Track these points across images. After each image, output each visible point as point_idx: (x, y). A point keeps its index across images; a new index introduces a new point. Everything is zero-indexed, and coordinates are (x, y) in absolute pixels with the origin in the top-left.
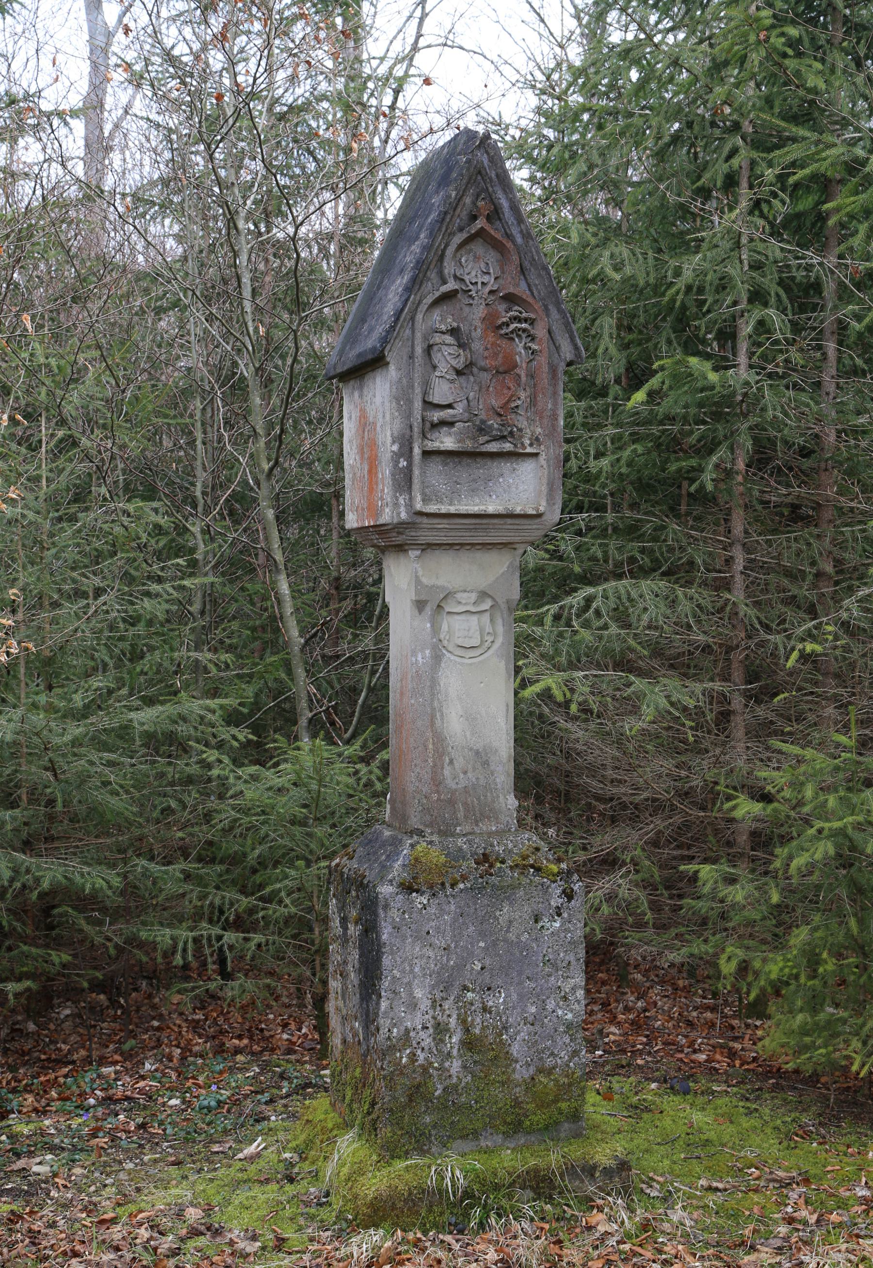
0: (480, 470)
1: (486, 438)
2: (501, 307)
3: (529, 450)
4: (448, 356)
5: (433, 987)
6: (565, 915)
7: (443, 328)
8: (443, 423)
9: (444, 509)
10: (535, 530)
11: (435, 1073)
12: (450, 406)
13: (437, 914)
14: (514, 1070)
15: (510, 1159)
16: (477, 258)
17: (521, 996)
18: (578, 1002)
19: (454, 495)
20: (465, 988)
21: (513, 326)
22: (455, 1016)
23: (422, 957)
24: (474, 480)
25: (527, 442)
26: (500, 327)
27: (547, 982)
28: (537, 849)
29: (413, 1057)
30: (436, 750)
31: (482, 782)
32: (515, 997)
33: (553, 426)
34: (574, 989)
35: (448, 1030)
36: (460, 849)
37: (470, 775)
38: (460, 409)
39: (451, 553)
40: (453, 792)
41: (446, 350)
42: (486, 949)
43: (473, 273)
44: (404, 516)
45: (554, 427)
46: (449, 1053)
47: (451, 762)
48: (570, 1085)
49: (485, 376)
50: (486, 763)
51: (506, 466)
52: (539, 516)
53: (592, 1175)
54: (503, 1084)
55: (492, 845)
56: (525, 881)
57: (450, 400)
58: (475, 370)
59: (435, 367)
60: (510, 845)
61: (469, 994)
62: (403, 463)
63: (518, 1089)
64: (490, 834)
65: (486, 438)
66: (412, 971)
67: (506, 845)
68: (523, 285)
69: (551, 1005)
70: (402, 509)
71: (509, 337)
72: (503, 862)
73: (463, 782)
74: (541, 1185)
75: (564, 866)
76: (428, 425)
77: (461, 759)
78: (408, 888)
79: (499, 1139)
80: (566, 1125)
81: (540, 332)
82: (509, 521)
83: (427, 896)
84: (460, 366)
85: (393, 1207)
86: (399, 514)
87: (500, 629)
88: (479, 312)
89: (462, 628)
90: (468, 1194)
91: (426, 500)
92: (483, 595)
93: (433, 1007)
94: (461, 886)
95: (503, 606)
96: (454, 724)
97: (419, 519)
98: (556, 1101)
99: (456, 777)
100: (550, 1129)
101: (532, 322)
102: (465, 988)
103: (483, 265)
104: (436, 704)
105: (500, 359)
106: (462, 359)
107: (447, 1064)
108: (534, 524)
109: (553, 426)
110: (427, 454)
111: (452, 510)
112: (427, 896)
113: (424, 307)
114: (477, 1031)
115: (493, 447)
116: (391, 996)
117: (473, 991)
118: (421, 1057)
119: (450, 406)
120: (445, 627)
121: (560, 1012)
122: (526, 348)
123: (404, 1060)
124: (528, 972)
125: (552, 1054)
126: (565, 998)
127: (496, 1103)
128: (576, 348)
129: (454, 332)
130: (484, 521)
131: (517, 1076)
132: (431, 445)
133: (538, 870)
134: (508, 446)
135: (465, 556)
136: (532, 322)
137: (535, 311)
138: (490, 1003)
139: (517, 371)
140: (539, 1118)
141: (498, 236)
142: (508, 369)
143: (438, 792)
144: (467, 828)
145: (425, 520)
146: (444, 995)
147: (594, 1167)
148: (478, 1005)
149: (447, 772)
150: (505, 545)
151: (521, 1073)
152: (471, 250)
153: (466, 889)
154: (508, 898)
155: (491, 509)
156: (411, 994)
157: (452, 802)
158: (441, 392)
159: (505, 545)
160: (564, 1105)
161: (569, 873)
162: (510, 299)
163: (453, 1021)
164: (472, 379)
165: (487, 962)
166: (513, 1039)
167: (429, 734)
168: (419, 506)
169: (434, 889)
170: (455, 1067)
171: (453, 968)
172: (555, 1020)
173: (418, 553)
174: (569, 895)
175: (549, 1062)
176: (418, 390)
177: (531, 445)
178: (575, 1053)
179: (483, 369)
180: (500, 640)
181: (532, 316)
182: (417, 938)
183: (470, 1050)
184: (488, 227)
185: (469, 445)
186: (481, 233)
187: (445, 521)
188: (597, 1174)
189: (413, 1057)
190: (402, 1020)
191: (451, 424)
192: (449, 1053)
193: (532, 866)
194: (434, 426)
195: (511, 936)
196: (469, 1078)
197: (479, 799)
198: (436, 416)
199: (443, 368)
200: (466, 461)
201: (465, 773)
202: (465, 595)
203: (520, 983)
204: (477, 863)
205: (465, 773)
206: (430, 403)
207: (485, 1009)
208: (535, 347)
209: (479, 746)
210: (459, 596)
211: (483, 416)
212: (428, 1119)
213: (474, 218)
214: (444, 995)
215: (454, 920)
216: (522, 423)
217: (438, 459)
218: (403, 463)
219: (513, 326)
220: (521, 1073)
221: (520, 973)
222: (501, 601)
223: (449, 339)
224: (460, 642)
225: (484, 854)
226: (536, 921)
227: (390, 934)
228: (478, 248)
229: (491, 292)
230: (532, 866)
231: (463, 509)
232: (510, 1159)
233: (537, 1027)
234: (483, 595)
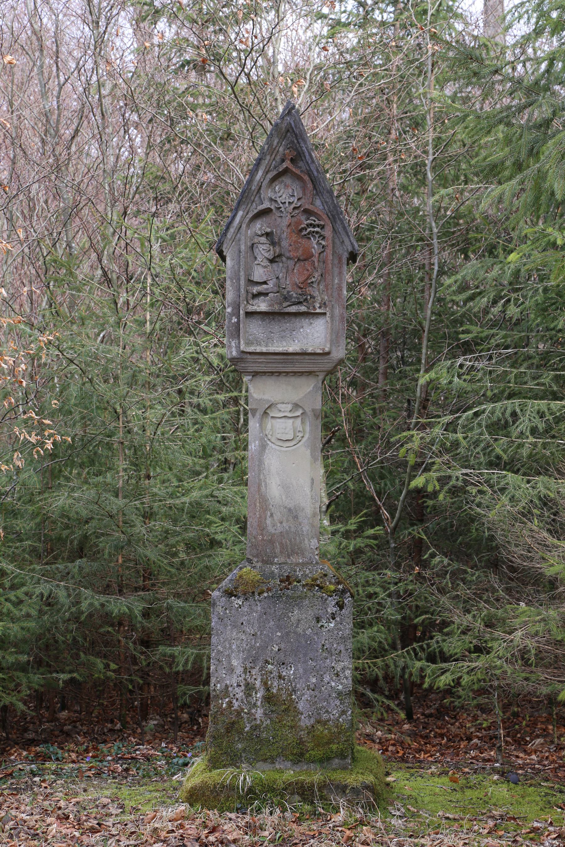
0: (287, 324)
1: (288, 303)
2: (303, 218)
3: (318, 311)
4: (264, 250)
5: (245, 659)
6: (338, 619)
7: (259, 233)
8: (259, 294)
9: (258, 349)
11: (245, 716)
12: (265, 283)
13: (250, 612)
14: (300, 719)
15: (289, 774)
16: (286, 186)
17: (305, 671)
18: (347, 678)
19: (269, 340)
20: (267, 662)
21: (309, 230)
22: (259, 680)
23: (238, 639)
24: (283, 331)
26: (301, 230)
27: (324, 662)
28: (325, 575)
29: (230, 704)
30: (261, 507)
31: (293, 529)
32: (301, 671)
33: (339, 294)
34: (343, 669)
35: (255, 688)
36: (273, 572)
37: (284, 524)
38: (271, 284)
39: (274, 378)
40: (273, 535)
42: (281, 637)
43: (284, 196)
44: (234, 353)
46: (255, 704)
47: (272, 515)
48: (339, 733)
49: (291, 263)
50: (296, 517)
51: (305, 322)
52: (328, 353)
53: (344, 792)
54: (292, 727)
55: (295, 571)
56: (310, 594)
57: (264, 279)
59: (256, 258)
60: (308, 571)
61: (270, 666)
62: (234, 320)
63: (302, 733)
64: (297, 564)
65: (288, 303)
66: (230, 647)
67: (305, 572)
68: (318, 202)
69: (327, 678)
70: (234, 349)
72: (298, 582)
73: (279, 528)
74: (305, 792)
75: (340, 587)
77: (279, 514)
78: (229, 594)
79: (289, 764)
80: (337, 761)
81: (328, 232)
82: (307, 357)
83: (242, 599)
84: (271, 257)
85: (203, 794)
86: (231, 352)
87: (308, 428)
88: (286, 221)
89: (281, 426)
90: (251, 790)
91: (248, 343)
92: (296, 406)
93: (245, 672)
94: (266, 595)
95: (309, 413)
96: (274, 491)
97: (245, 356)
98: (328, 743)
99: (275, 525)
100: (325, 760)
101: (323, 227)
102: (267, 662)
103: (290, 191)
104: (262, 476)
105: (300, 252)
106: (272, 252)
107: (253, 711)
108: (325, 359)
110: (249, 314)
111: (264, 350)
112: (242, 599)
113: (247, 220)
114: (275, 691)
115: (293, 309)
116: (217, 663)
117: (272, 664)
118: (236, 704)
119: (265, 283)
120: (269, 426)
121: (333, 684)
122: (318, 243)
123: (224, 705)
124: (311, 655)
125: (327, 711)
126: (337, 675)
127: (287, 740)
128: (352, 244)
130: (290, 357)
131: (302, 724)
132: (250, 309)
133: (321, 588)
134: (303, 309)
135: (283, 379)
136: (323, 227)
137: (323, 220)
138: (284, 674)
139: (313, 259)
140: (317, 753)
141: (298, 172)
142: (307, 257)
143: (262, 535)
144: (282, 560)
145: (249, 356)
146: (252, 665)
147: (346, 786)
148: (275, 674)
149: (269, 521)
151: (305, 722)
153: (268, 596)
154: (297, 605)
155: (291, 350)
156: (229, 662)
157: (271, 542)
158: (258, 274)
160: (334, 747)
161: (344, 592)
162: (308, 212)
163: (258, 683)
164: (281, 265)
165: (283, 646)
166: (299, 698)
167: (257, 496)
168: (242, 348)
169: (247, 595)
170: (259, 713)
171: (259, 648)
172: (329, 689)
173: (250, 377)
174: (341, 606)
175: (325, 717)
176: (242, 273)
177: (320, 307)
178: (343, 712)
179: (288, 258)
180: (307, 436)
181: (322, 223)
182: (234, 626)
183: (269, 703)
184: (291, 167)
185: (276, 308)
186: (286, 171)
188: (348, 791)
189: (230, 704)
190: (223, 679)
191: (266, 294)
192: (255, 704)
193: (318, 586)
194: (255, 296)
195: (300, 630)
196: (269, 722)
197: (290, 541)
199: (260, 258)
201: (281, 523)
202: (284, 405)
203: (305, 662)
204: (281, 581)
205: (281, 523)
207: (280, 677)
208: (323, 243)
209: (291, 505)
210: (279, 406)
211: (289, 288)
212: (240, 746)
213: (283, 161)
214: (252, 665)
215: (260, 617)
216: (316, 294)
217: (258, 317)
218: (234, 320)
219: (309, 230)
220: (305, 722)
221: (305, 655)
222: (308, 410)
223: (263, 239)
224: (279, 436)
225: (288, 577)
226: (318, 622)
227: (216, 622)
228: (287, 180)
229: (295, 208)
230: (318, 586)
231: (272, 349)
232: (289, 774)
233: (316, 693)
234: (296, 406)
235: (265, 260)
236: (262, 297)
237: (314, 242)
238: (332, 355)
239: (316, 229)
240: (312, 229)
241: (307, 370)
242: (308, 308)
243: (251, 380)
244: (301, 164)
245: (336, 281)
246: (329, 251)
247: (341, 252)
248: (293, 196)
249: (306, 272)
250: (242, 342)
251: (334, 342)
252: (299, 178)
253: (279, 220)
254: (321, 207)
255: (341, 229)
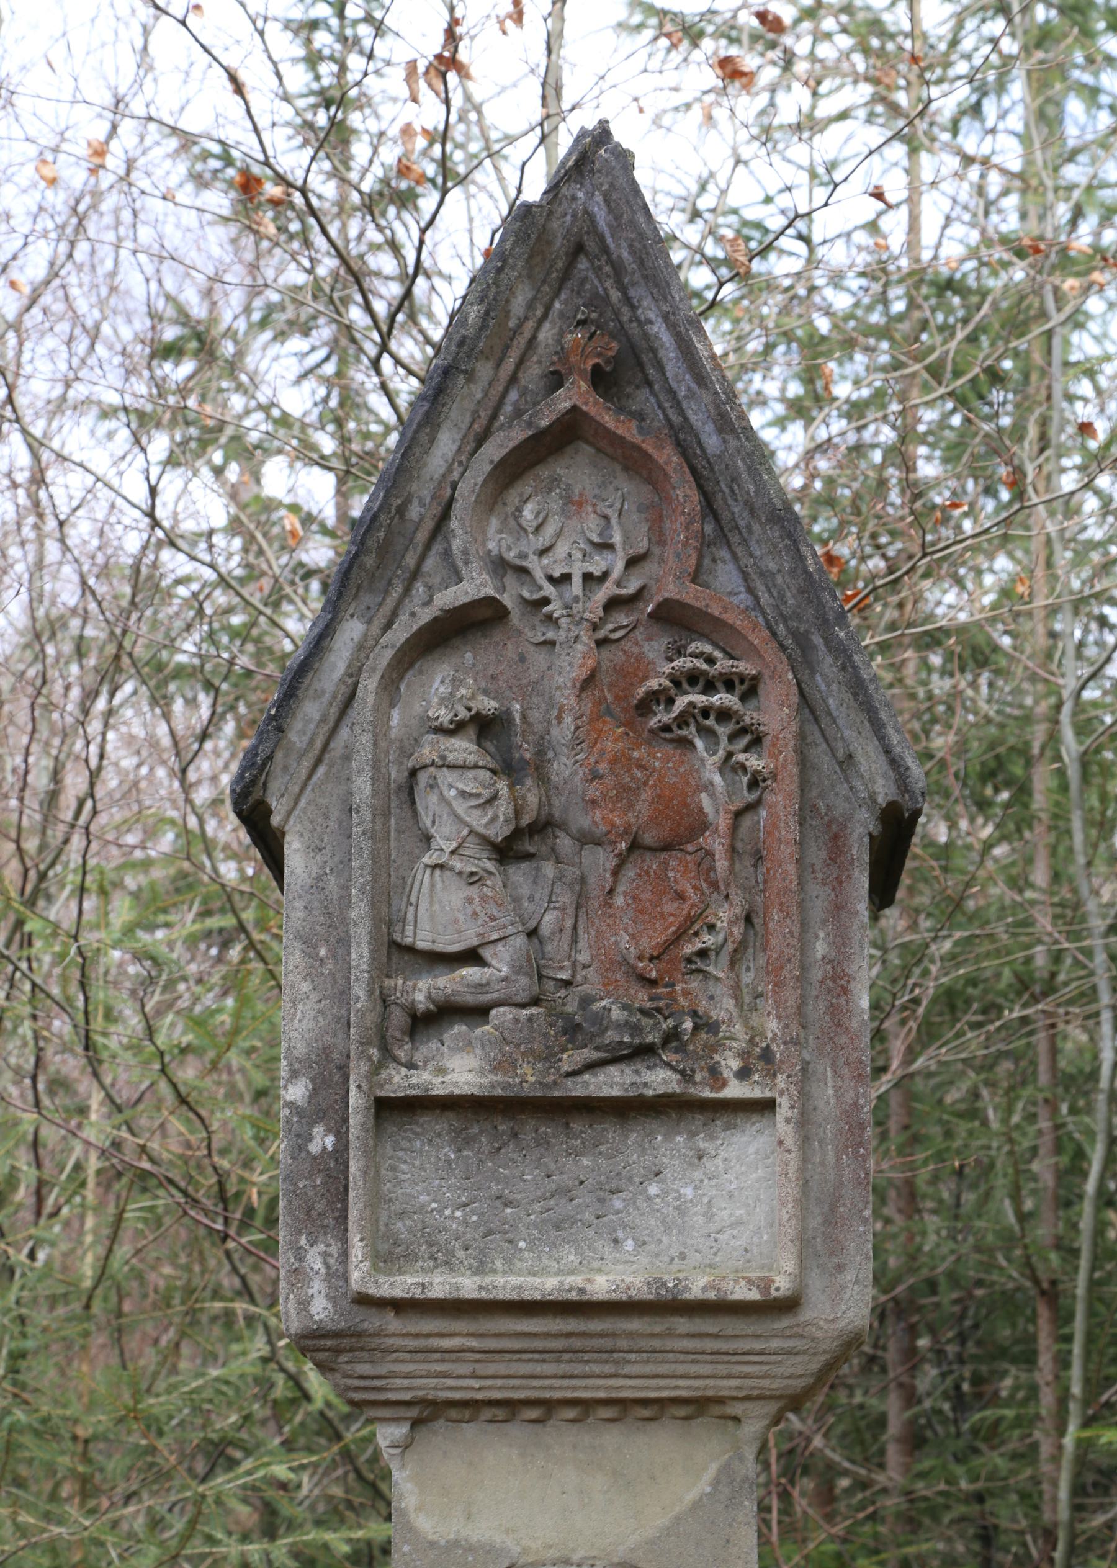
0: (581, 1157)
3: (735, 1090)
4: (462, 802)
9: (439, 1285)
10: (783, 1359)
12: (472, 957)
19: (491, 1241)
25: (731, 1063)
26: (644, 707)
33: (834, 1011)
38: (501, 963)
41: (452, 784)
43: (561, 550)
44: (320, 1308)
45: (838, 1015)
51: (670, 1145)
52: (788, 1305)
58: (564, 843)
59: (428, 838)
70: (317, 1286)
71: (674, 737)
76: (398, 1018)
81: (774, 713)
82: (683, 1324)
84: (499, 832)
88: (573, 661)
91: (386, 1258)
97: (372, 1321)
103: (592, 527)
105: (643, 807)
106: (503, 808)
108: (773, 1334)
109: (834, 1011)
110: (390, 1110)
111: (469, 1286)
115: (612, 1082)
119: (472, 957)
122: (729, 766)
128: (894, 762)
129: (484, 727)
130: (595, 1325)
132: (400, 1082)
134: (659, 1080)
135: (563, 1438)
136: (750, 688)
137: (754, 652)
141: (629, 431)
142: (676, 833)
145: (393, 1323)
150: (699, 1406)
152: (555, 480)
155: (601, 1286)
158: (441, 913)
159: (699, 1406)
162: (674, 618)
164: (549, 869)
168: (359, 1276)
173: (399, 1431)
176: (359, 911)
177: (743, 1074)
179: (586, 839)
181: (746, 667)
185: (528, 1078)
187: (461, 1325)
191: (479, 1013)
198: (424, 989)
200: (530, 1128)
206: (411, 950)
208: (754, 762)
213: (556, 380)
216: (723, 1008)
217: (438, 1125)
218: (322, 1140)
219: (681, 702)
223: (462, 748)
228: (577, 471)
229: (613, 604)
231: (506, 1284)
235: (471, 848)
236: (459, 1028)
237: (707, 760)
238: (806, 1314)
239: (720, 699)
240: (700, 699)
241: (684, 1388)
242: (687, 1077)
243: (406, 1446)
244: (642, 399)
245: (820, 949)
246: (781, 801)
247: (841, 808)
248: (606, 546)
249: (670, 907)
250: (357, 1249)
251: (816, 1245)
252: (634, 462)
253: (539, 659)
254: (743, 598)
255: (836, 700)
